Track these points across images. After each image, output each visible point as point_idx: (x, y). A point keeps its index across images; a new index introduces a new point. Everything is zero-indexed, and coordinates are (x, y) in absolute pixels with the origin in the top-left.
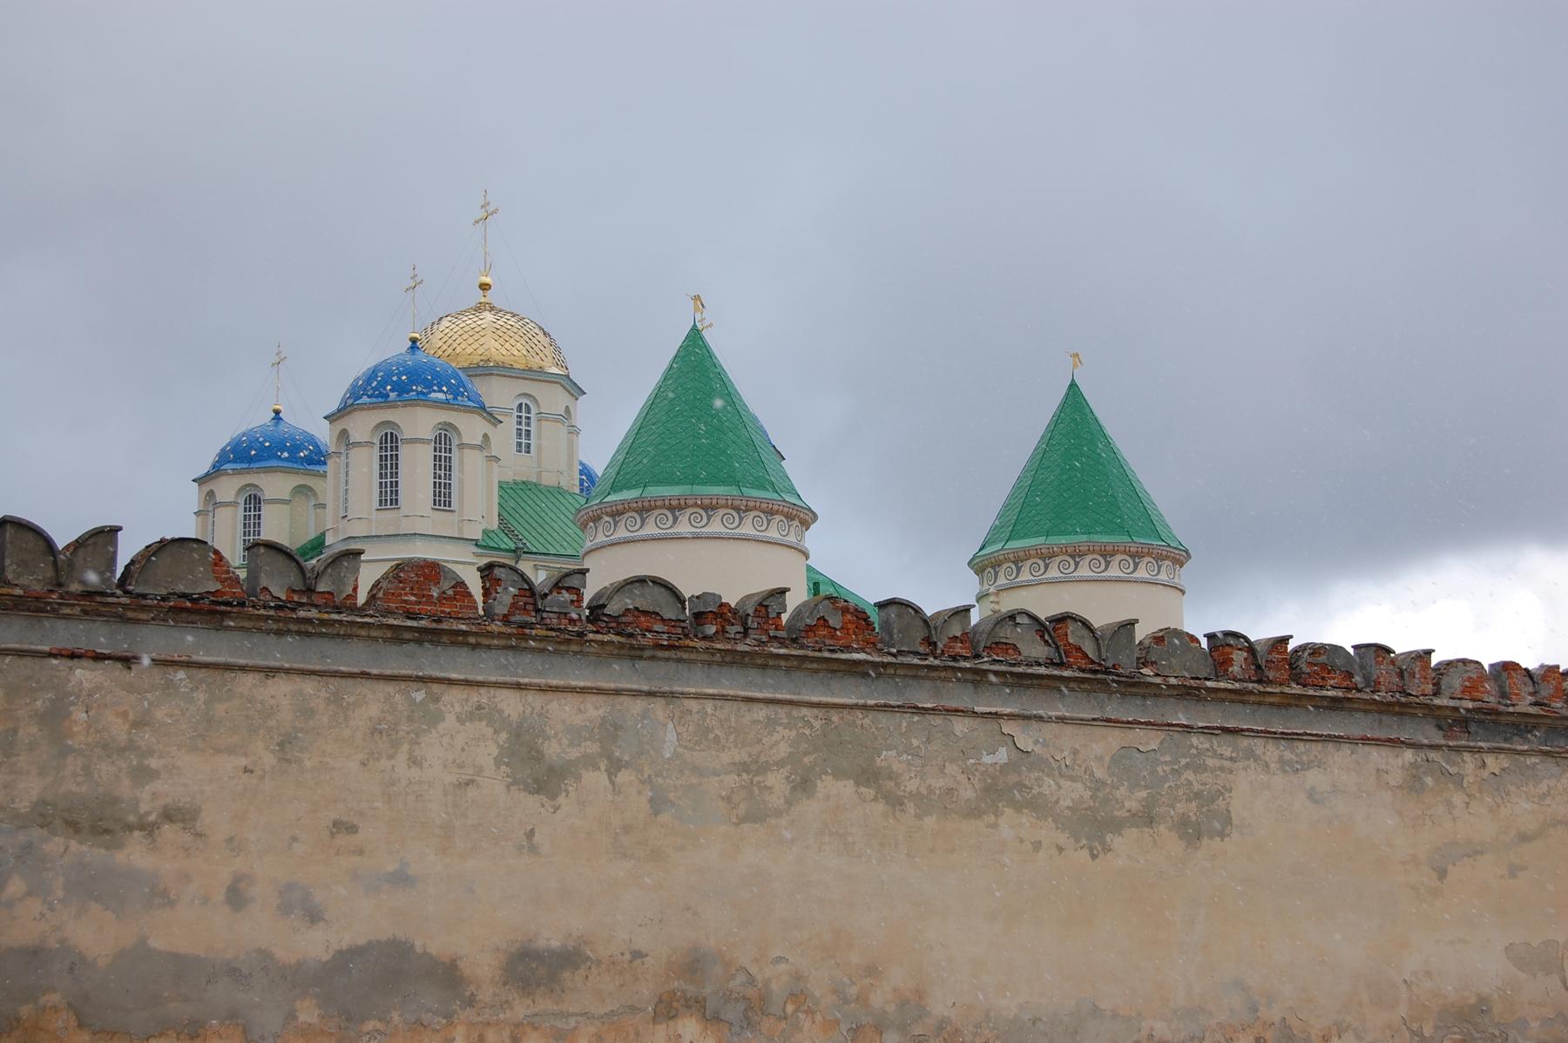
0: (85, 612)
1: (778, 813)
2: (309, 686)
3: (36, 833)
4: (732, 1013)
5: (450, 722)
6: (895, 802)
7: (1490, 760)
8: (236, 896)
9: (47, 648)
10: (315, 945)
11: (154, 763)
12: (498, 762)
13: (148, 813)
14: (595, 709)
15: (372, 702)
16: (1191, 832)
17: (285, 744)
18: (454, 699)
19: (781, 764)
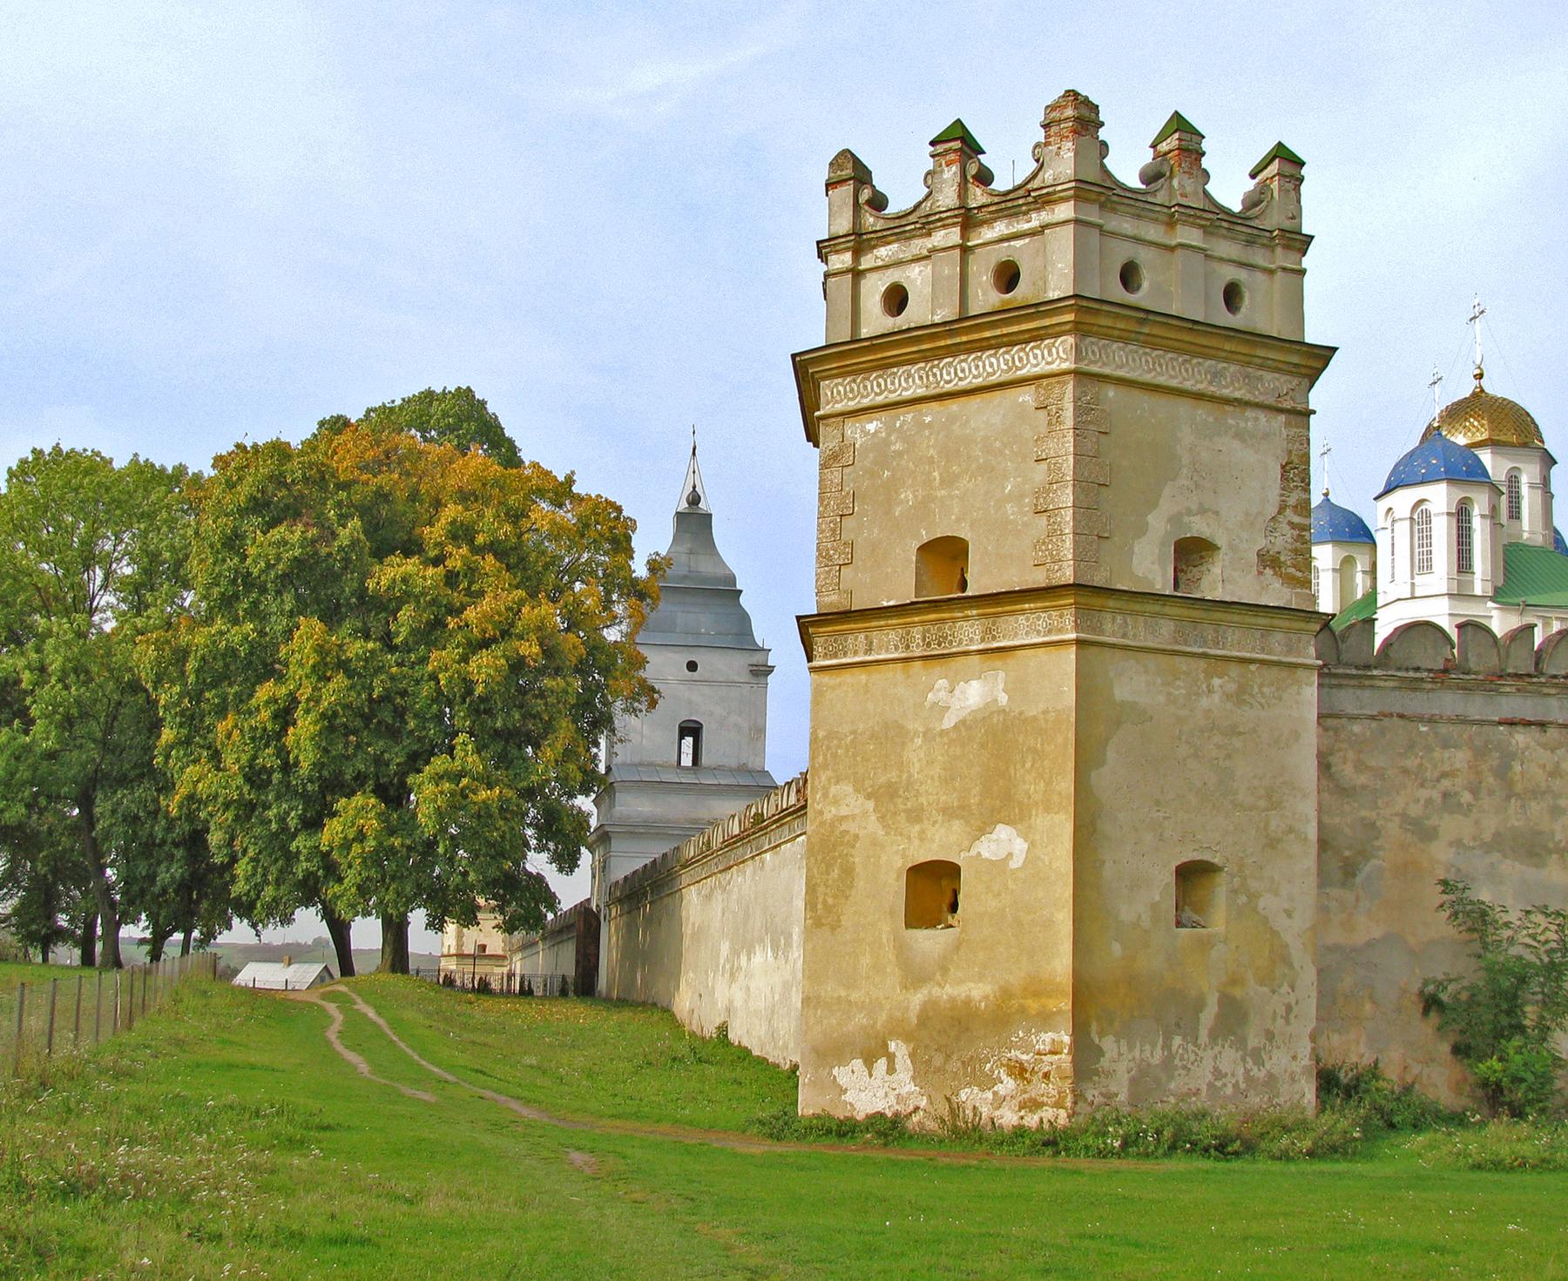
0: (1518, 690)
9: (1497, 719)
13: (1561, 841)
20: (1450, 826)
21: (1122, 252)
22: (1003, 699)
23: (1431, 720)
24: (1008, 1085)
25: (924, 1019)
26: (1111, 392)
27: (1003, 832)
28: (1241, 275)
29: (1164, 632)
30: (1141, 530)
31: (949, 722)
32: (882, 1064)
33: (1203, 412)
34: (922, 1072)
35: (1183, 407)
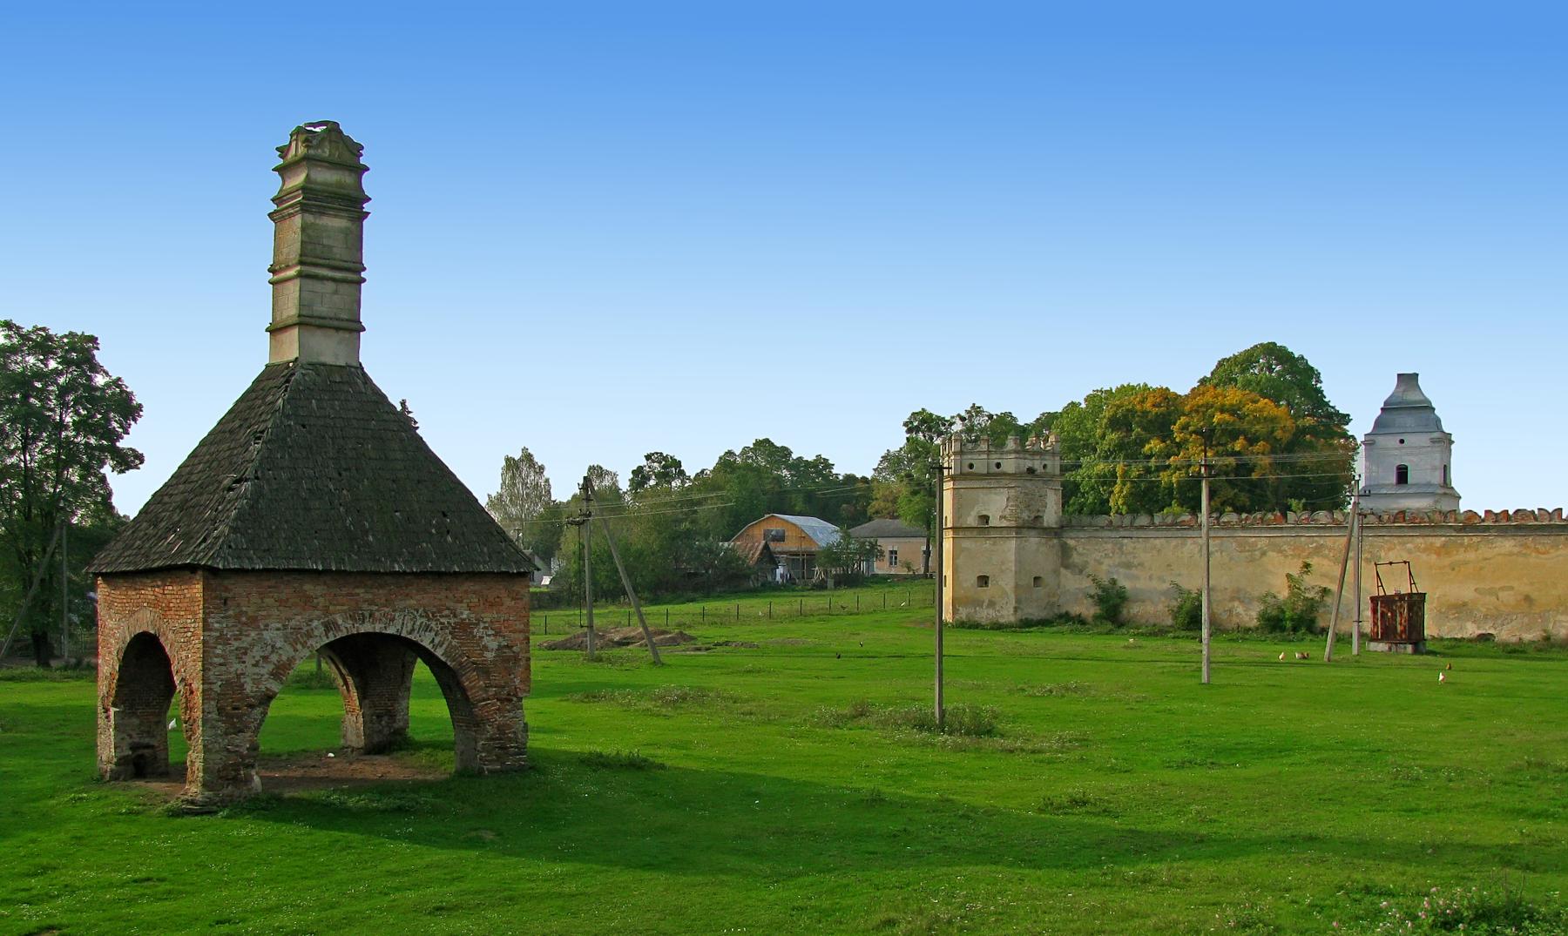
1: (1258, 560)
2: (1162, 540)
6: (1286, 556)
7: (1474, 539)
8: (1151, 578)
15: (1174, 542)
18: (1189, 541)
20: (1107, 561)
23: (1102, 538)
26: (962, 490)
28: (999, 461)
29: (975, 533)
30: (969, 515)
33: (985, 491)
35: (980, 490)
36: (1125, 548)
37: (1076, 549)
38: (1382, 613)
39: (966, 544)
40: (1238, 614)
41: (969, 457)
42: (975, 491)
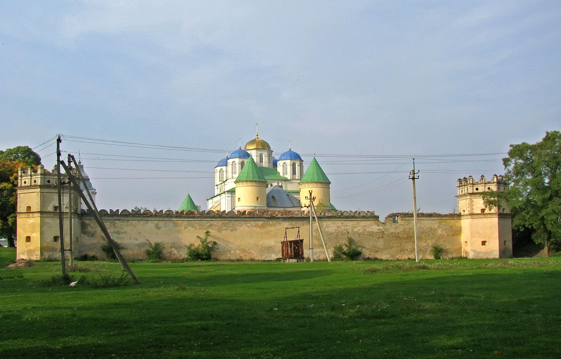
2: (136, 221)
3: (113, 234)
4: (178, 248)
5: (149, 224)
7: (274, 222)
10: (138, 242)
11: (123, 228)
12: (155, 227)
14: (164, 222)
15: (142, 222)
16: (232, 231)
17: (135, 226)
18: (150, 222)
19: (183, 226)
21: (47, 180)
22: (34, 222)
24: (35, 256)
25: (28, 251)
26: (45, 193)
27: (34, 234)
29: (52, 215)
31: (29, 223)
32: (24, 255)
34: (28, 255)
36: (116, 224)
37: (90, 225)
38: (294, 248)
39: (47, 220)
40: (174, 254)
41: (48, 177)
42: (52, 194)
